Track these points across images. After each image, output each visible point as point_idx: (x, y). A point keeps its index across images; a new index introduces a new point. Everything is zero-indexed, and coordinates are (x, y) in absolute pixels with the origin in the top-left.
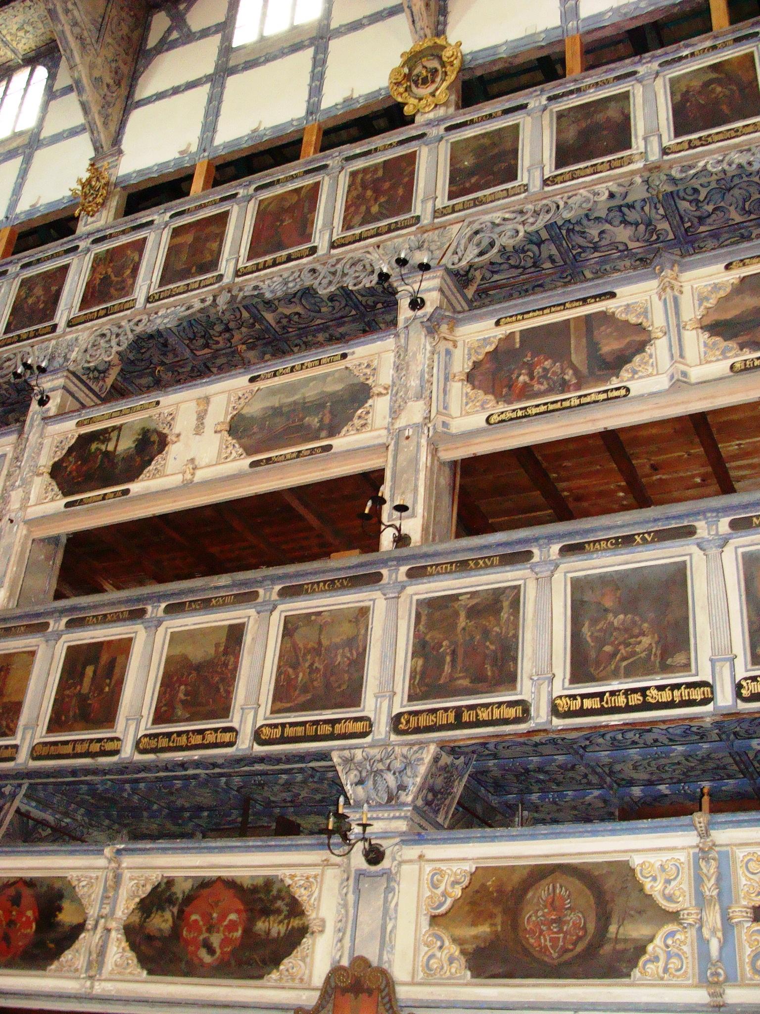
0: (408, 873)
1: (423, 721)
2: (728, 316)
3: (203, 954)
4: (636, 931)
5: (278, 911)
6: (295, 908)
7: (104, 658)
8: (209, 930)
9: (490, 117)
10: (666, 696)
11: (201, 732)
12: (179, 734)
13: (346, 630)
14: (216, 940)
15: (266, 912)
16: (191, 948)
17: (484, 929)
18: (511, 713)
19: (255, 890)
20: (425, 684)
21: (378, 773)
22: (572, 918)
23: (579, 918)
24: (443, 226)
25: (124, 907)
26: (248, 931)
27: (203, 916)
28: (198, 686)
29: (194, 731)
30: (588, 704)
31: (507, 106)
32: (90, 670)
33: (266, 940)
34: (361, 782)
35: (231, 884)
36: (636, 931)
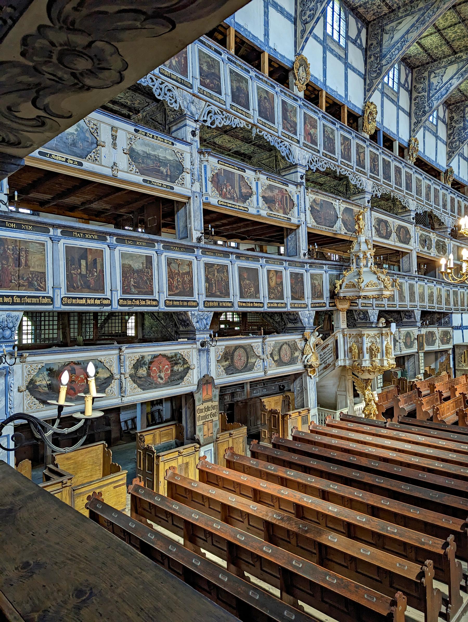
0: (212, 349)
1: (211, 304)
2: (266, 195)
3: (159, 380)
4: (253, 360)
5: (180, 363)
6: (185, 362)
7: (90, 257)
8: (160, 372)
9: (210, 47)
10: (256, 305)
11: (145, 300)
12: (136, 300)
13: (186, 269)
14: (162, 375)
15: (176, 364)
16: (155, 379)
17: (227, 363)
18: (230, 305)
19: (172, 357)
20: (209, 293)
21: (202, 319)
22: (243, 358)
23: (244, 359)
24: (200, 98)
25: (128, 369)
26: (172, 371)
27: (157, 367)
28: (137, 278)
29: (142, 299)
30: (244, 304)
31: (216, 47)
32: (83, 262)
33: (178, 373)
34: (197, 322)
35: (164, 356)
36: (253, 360)
